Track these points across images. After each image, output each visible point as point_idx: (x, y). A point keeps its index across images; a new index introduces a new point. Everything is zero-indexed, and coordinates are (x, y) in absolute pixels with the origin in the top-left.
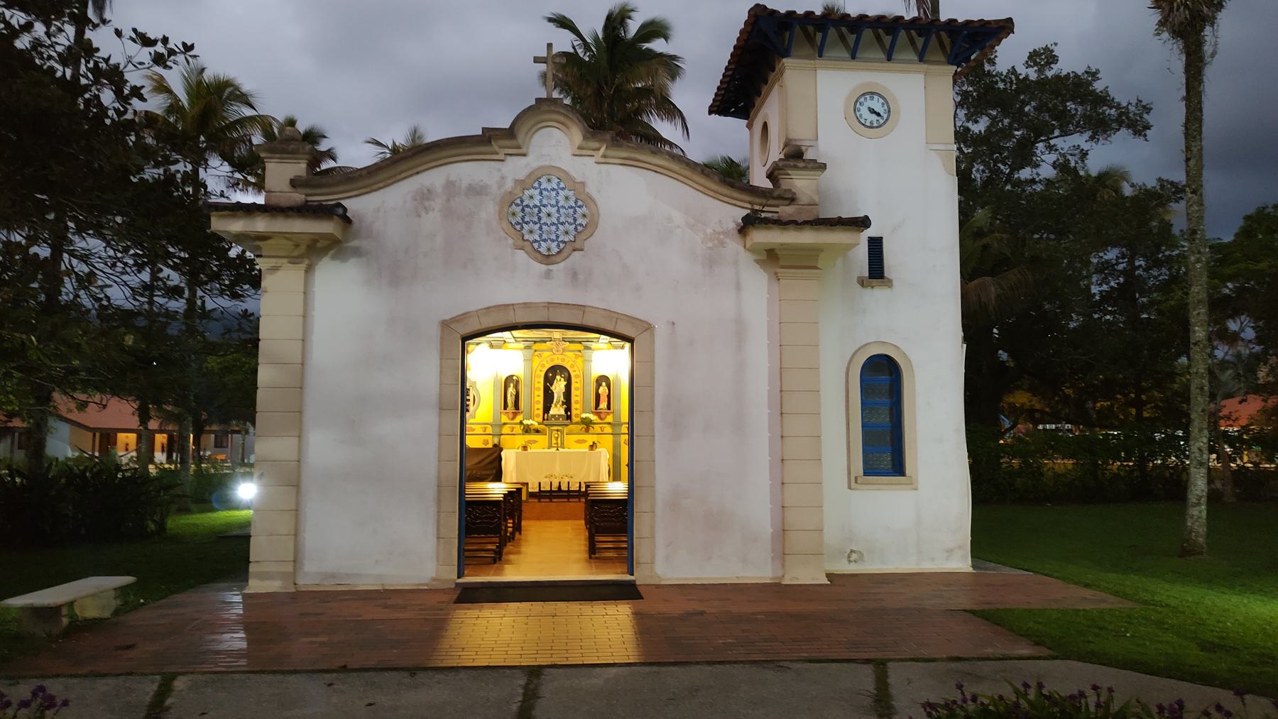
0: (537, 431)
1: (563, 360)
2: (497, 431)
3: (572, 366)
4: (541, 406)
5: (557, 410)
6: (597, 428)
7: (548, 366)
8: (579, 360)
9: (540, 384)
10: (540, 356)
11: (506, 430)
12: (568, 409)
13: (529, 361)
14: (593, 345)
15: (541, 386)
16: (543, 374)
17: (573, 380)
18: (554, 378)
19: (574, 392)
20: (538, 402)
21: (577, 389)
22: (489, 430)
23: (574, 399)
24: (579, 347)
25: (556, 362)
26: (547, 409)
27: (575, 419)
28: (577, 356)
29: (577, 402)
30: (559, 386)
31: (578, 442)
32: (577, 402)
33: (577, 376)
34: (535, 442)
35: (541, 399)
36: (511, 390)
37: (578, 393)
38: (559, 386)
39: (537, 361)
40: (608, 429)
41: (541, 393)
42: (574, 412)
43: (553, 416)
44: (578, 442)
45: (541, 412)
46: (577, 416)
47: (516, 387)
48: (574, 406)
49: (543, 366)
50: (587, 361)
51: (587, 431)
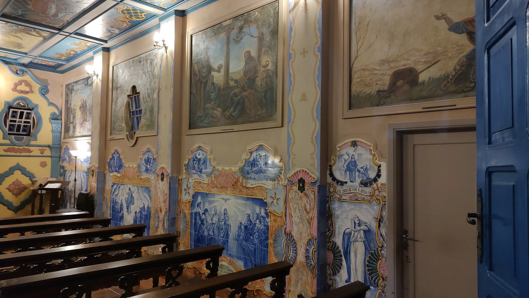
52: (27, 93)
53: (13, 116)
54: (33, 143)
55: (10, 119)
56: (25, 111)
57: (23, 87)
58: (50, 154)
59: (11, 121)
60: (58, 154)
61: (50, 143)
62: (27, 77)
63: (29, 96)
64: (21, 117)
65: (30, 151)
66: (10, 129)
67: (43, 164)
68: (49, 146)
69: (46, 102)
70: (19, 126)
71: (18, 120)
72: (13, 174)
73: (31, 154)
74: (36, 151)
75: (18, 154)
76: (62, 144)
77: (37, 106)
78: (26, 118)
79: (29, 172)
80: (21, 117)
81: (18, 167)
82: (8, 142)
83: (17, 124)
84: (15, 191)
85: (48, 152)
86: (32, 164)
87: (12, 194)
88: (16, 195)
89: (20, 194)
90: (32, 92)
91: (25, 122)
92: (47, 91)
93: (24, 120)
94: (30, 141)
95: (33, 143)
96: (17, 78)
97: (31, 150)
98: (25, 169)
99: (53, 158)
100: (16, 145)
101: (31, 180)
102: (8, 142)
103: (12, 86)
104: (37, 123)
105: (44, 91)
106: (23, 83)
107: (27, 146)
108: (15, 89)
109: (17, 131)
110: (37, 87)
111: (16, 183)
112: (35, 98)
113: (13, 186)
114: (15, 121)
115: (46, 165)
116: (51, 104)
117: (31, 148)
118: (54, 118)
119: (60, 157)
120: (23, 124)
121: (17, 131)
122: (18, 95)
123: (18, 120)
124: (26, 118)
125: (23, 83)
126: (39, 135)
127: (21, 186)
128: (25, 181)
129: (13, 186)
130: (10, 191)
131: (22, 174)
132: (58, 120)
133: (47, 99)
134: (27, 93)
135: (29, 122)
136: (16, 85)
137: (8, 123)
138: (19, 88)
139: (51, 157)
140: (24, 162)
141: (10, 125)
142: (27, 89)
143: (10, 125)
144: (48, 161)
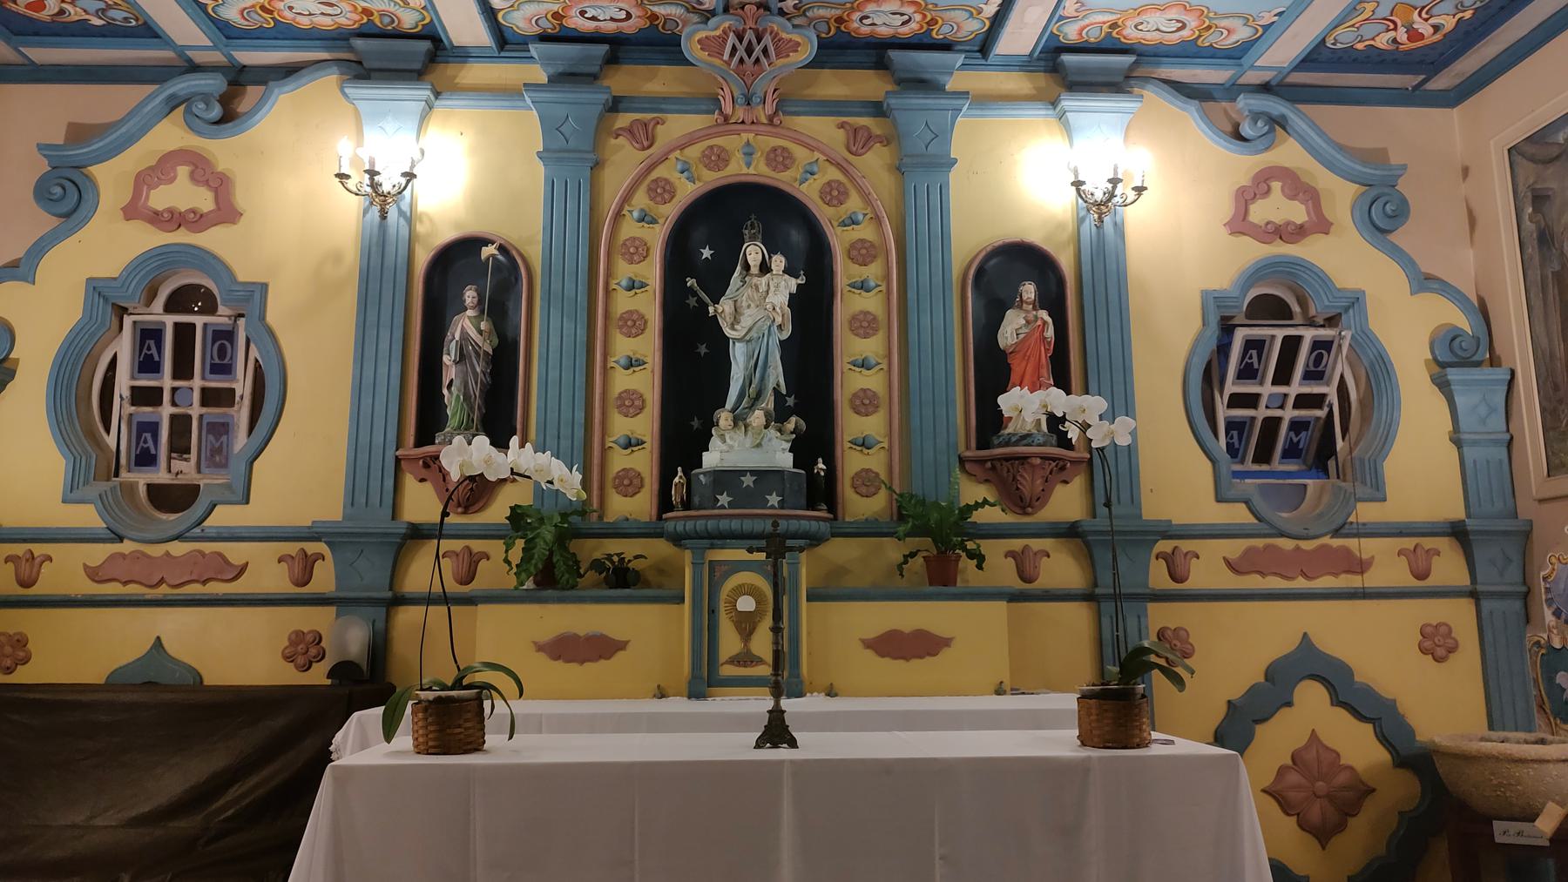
0: (621, 580)
1: (780, 159)
2: (371, 575)
3: (834, 193)
4: (647, 425)
5: (744, 445)
6: (999, 566)
7: (687, 191)
8: (874, 163)
9: (639, 287)
10: (644, 136)
11: (420, 573)
12: (815, 443)
13: (573, 159)
14: (957, 81)
15: (650, 305)
16: (657, 237)
17: (844, 271)
18: (728, 260)
19: (849, 346)
20: (631, 404)
21: (864, 325)
22: (324, 579)
23: (849, 382)
24: (869, 85)
25: (738, 170)
26: (683, 438)
27: (859, 506)
28: (859, 141)
29: (865, 403)
30: (756, 306)
31: (894, 645)
32: (865, 403)
33: (862, 253)
34: (600, 648)
35: (647, 383)
36: (467, 326)
37: (870, 347)
38: (756, 306)
39: (623, 161)
40: (1061, 567)
41: (649, 345)
42: (852, 462)
43: (726, 479)
44: (894, 645)
45: (644, 462)
46: (867, 484)
47: (498, 309)
48: (850, 425)
49: (662, 191)
50: (924, 166)
51: (941, 578)
52: (1296, 233)
53: (1247, 373)
54: (1367, 512)
55: (1231, 387)
56: (1309, 335)
57: (1277, 208)
58: (1461, 578)
59: (1237, 401)
60: (1514, 573)
61: (1457, 512)
62: (1288, 153)
63: (1311, 251)
64: (1282, 377)
65: (1360, 566)
66: (1232, 451)
67: (1437, 644)
68: (1458, 532)
69: (1394, 274)
70: (1272, 424)
71: (1267, 389)
72: (1289, 704)
73: (1373, 580)
74: (1387, 564)
75: (1300, 583)
76: (1526, 509)
77: (1356, 301)
78: (1309, 376)
79: (1369, 693)
80: (1282, 377)
81: (1308, 664)
82: (1239, 514)
83: (1261, 413)
84: (1315, 813)
85: (1449, 567)
86: (1375, 641)
87: (1302, 825)
88: (1323, 834)
89: (1340, 827)
90: (1321, 225)
91: (1303, 401)
92: (1400, 213)
93: (1296, 387)
94: (1351, 500)
95: (1367, 512)
96: (1243, 165)
97: (1364, 556)
98: (1345, 670)
99: (1487, 605)
100: (1282, 535)
101: (1383, 738)
102: (1239, 514)
103: (1227, 209)
104: (1361, 402)
105: (1383, 214)
106: (1276, 186)
107: (1336, 533)
108: (1240, 225)
109: (1256, 460)
110: (1341, 195)
111: (1312, 759)
112: (1345, 259)
113: (1294, 778)
114: (1251, 401)
115: (1452, 650)
116: (1424, 282)
117: (1367, 547)
118: (1455, 357)
119: (1526, 596)
120: (1289, 414)
121: (1256, 460)
122: (1253, 251)
123: (1267, 389)
124: (1309, 376)
125: (1276, 186)
126: (1395, 467)
127: (1342, 778)
128: (1359, 748)
129: (1294, 778)
130: (1286, 807)
131: (1337, 701)
132: (1478, 364)
133: (1397, 253)
134: (1296, 233)
135: (1316, 401)
136: (1245, 197)
137: (1222, 412)
138: (1260, 212)
139: (1474, 594)
140: (1343, 631)
141: (1231, 425)
142: (1297, 213)
143: (1231, 425)
144: (1460, 617)
